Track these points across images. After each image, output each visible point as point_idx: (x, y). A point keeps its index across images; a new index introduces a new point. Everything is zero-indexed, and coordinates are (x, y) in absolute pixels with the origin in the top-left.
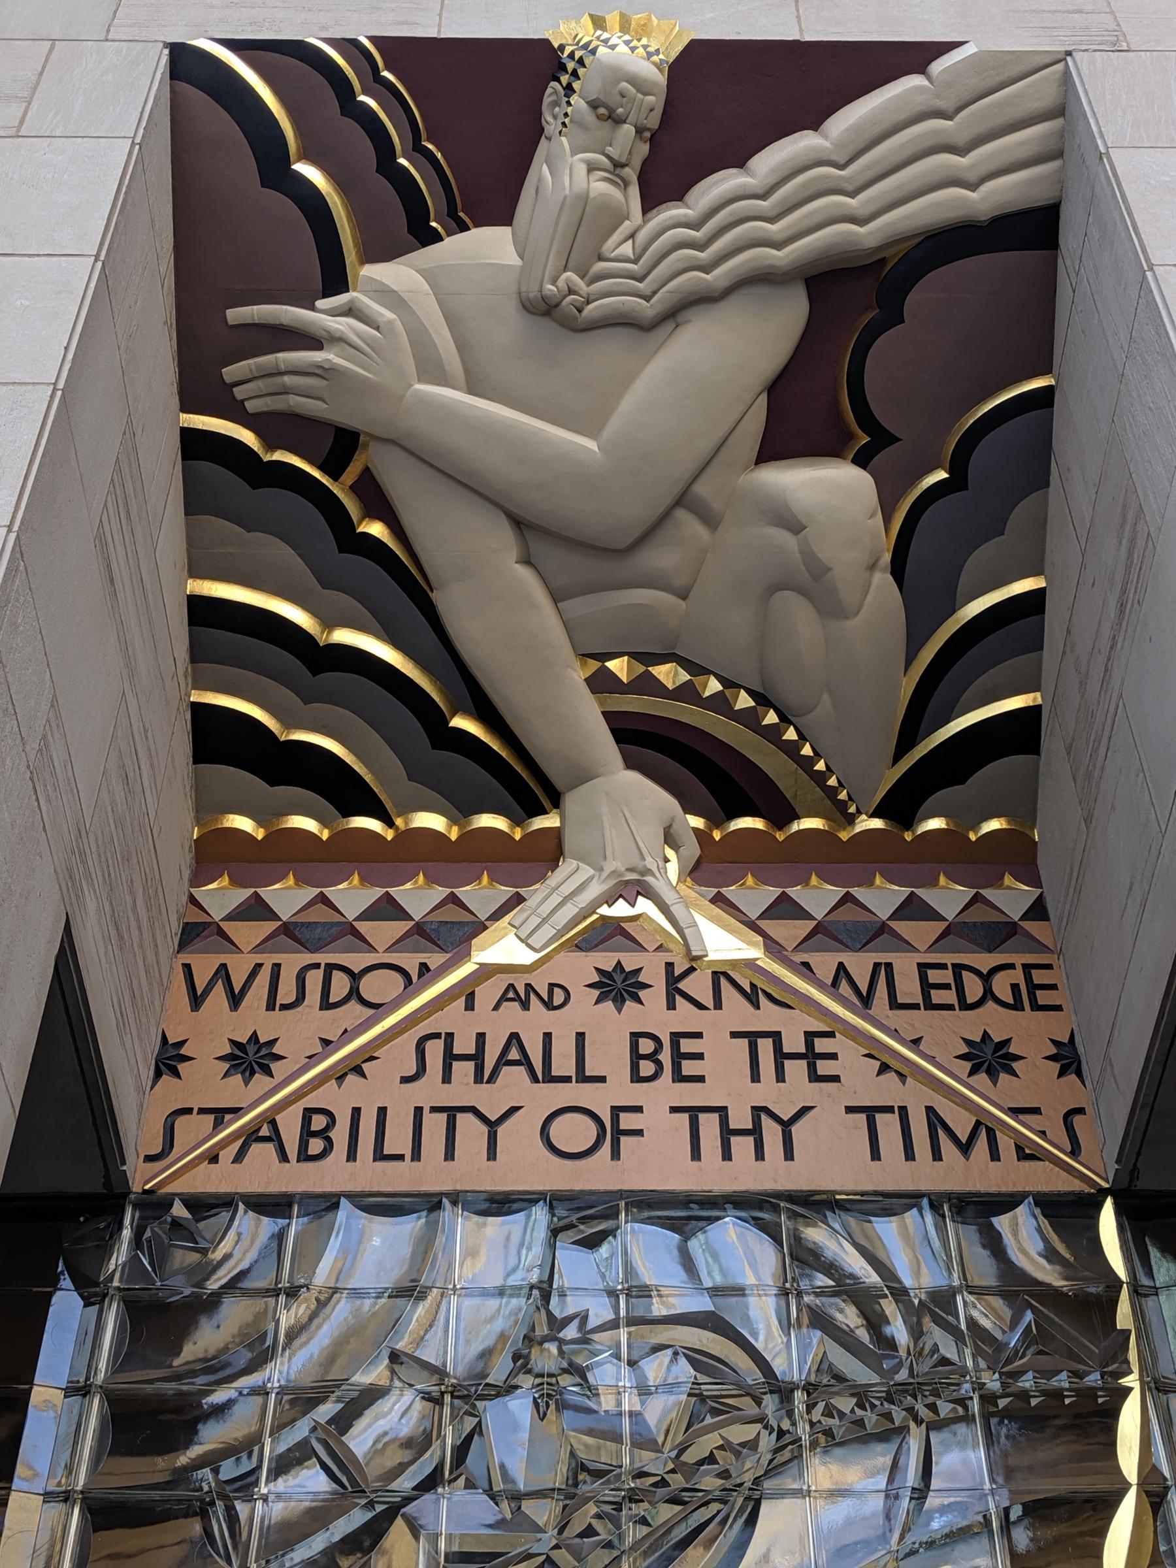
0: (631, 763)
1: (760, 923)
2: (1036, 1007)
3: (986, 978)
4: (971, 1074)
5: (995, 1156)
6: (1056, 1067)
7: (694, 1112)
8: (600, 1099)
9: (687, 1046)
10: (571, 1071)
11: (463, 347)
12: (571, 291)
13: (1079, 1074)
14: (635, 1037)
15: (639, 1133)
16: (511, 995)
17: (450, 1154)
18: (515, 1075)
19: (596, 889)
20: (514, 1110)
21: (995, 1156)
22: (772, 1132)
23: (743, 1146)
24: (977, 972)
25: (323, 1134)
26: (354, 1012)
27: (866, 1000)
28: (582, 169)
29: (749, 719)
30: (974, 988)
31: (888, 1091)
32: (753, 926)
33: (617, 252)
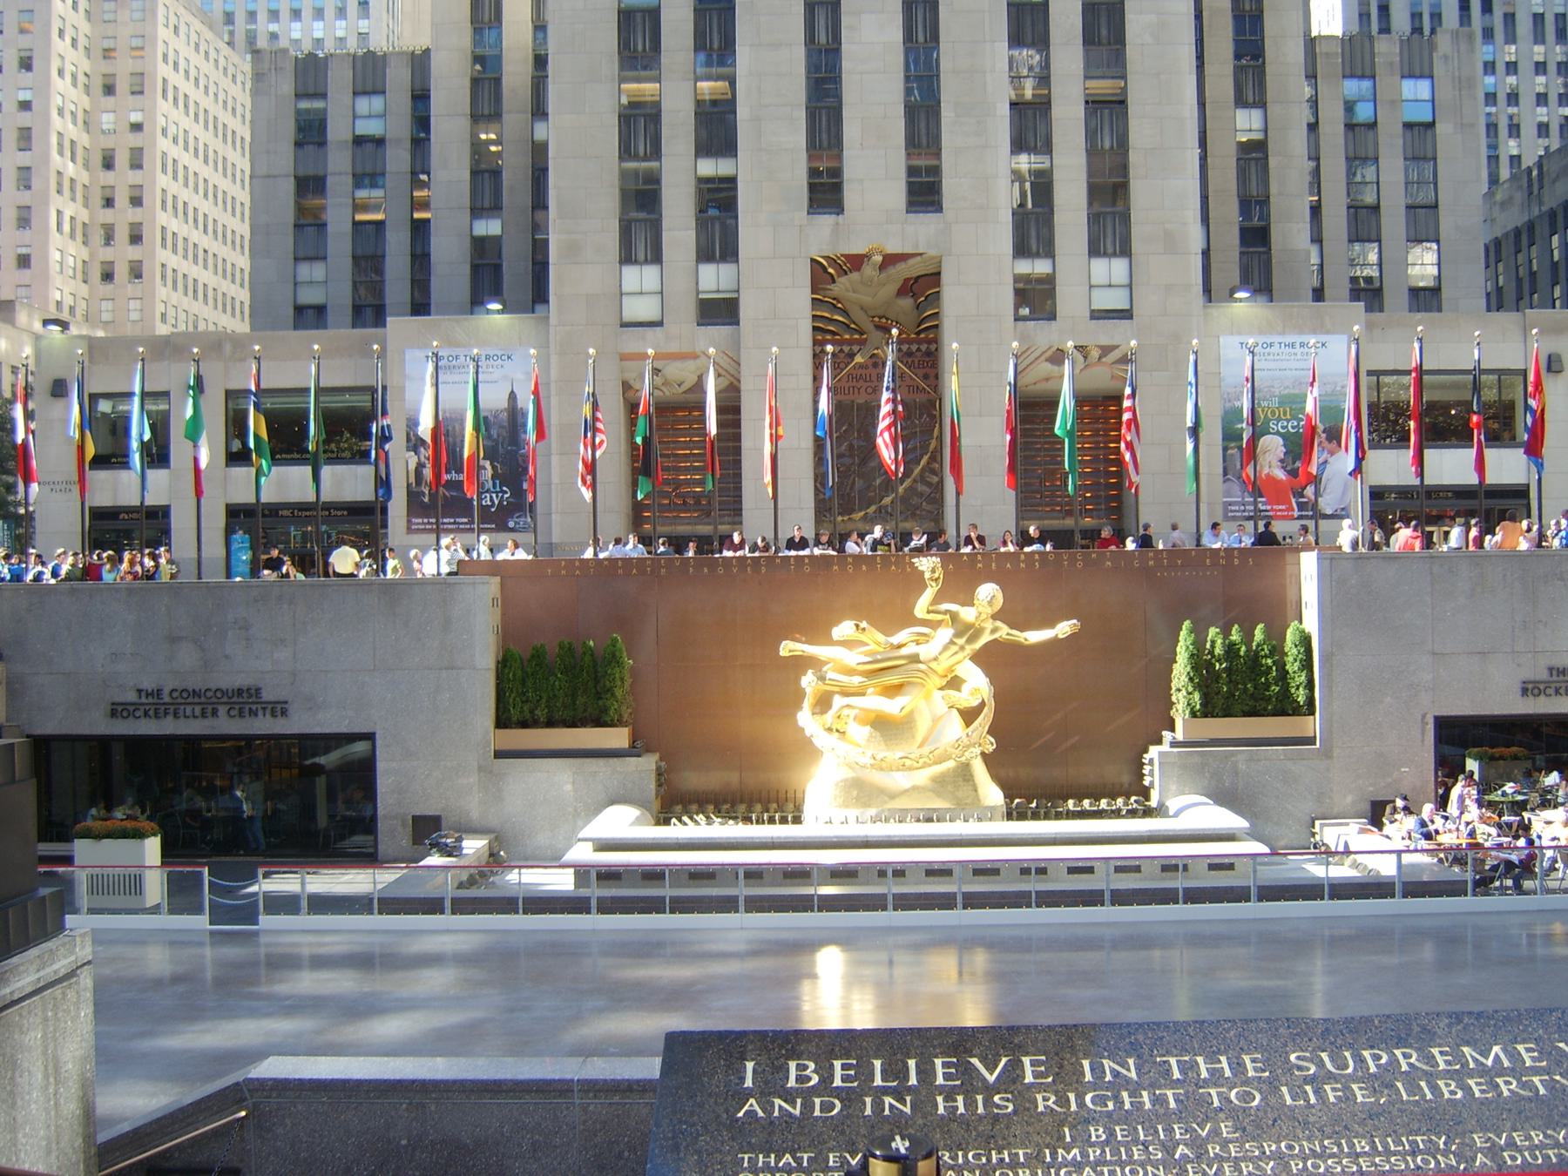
8: (873, 385)
26: (839, 370)
31: (911, 383)
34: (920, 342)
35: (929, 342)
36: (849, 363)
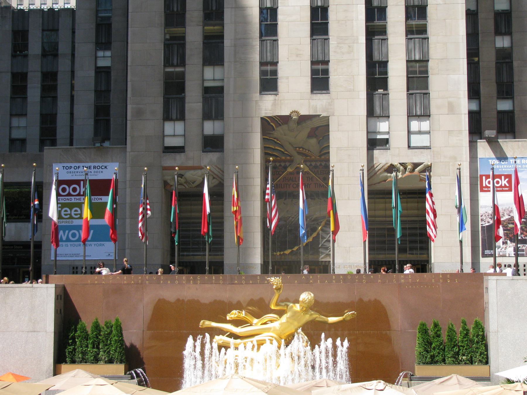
0: (298, 155)
23: (306, 187)
25: (278, 186)
30: (324, 172)
32: (308, 166)
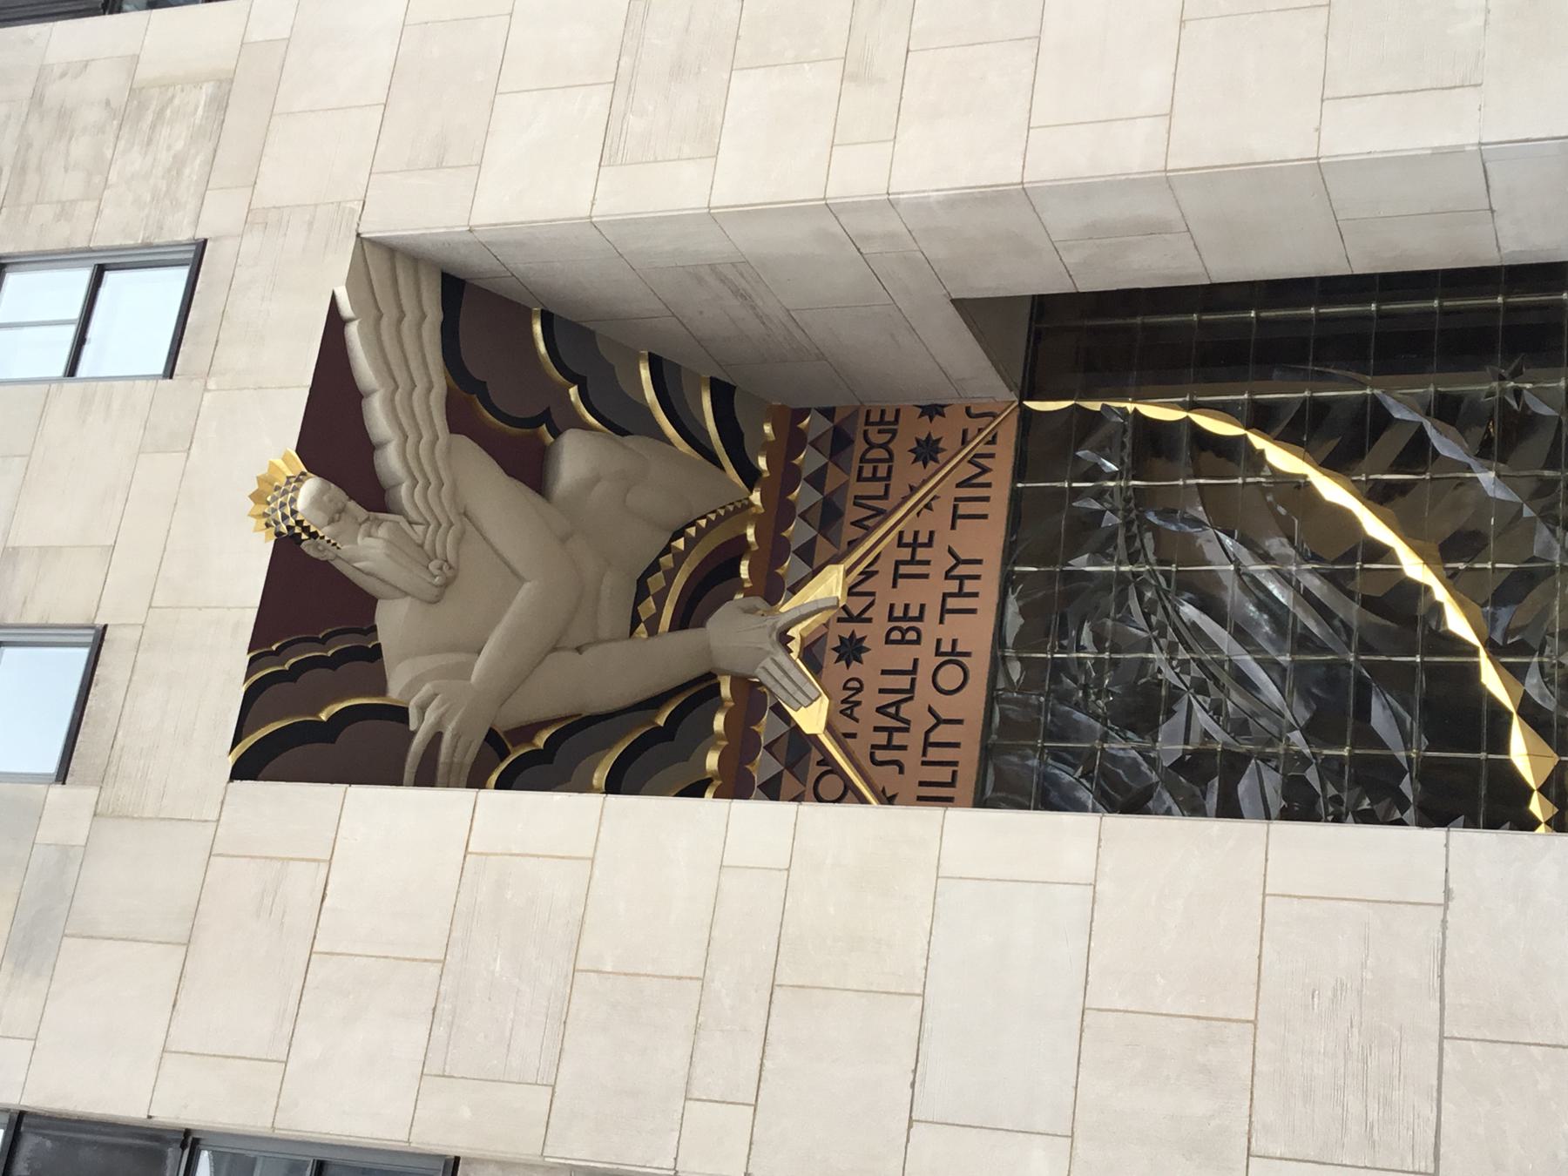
0: (701, 624)
1: (815, 566)
2: (896, 421)
3: (872, 446)
4: (936, 461)
5: (992, 456)
6: (937, 418)
7: (944, 611)
8: (929, 662)
9: (898, 612)
10: (909, 678)
11: (453, 648)
12: (441, 568)
13: (943, 406)
14: (888, 641)
15: (954, 642)
16: (849, 712)
17: (957, 745)
18: (905, 710)
19: (781, 657)
20: (930, 710)
21: (992, 456)
22: (962, 570)
23: (969, 586)
24: (867, 451)
27: (879, 512)
28: (369, 541)
29: (691, 544)
30: (880, 453)
31: (944, 510)
32: (815, 573)
33: (420, 533)
34: (788, 476)
35: (793, 440)
36: (827, 759)
